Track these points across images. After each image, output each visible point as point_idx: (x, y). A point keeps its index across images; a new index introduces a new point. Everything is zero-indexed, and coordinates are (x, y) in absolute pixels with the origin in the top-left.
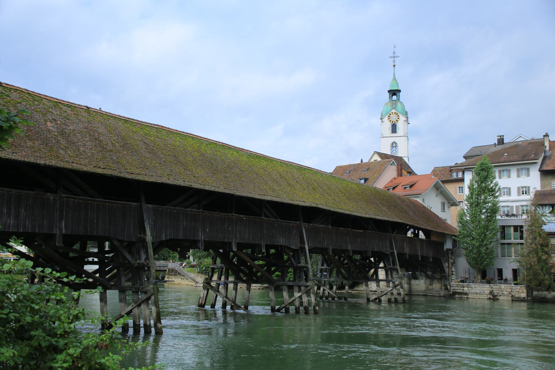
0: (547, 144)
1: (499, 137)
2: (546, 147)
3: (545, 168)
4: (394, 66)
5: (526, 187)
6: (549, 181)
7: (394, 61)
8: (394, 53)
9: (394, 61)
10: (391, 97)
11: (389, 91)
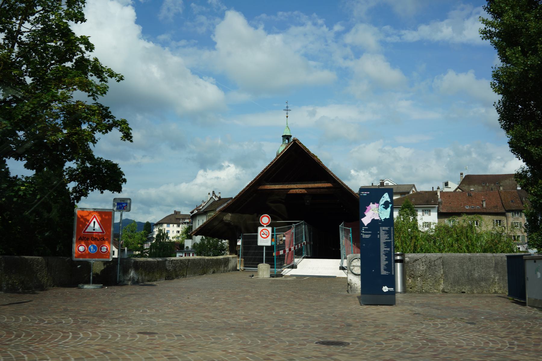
0: (439, 194)
1: (381, 181)
2: (438, 196)
3: (441, 211)
4: (287, 117)
5: (428, 223)
6: (443, 219)
7: (287, 114)
8: (287, 107)
9: (287, 114)
10: (284, 141)
11: (283, 136)
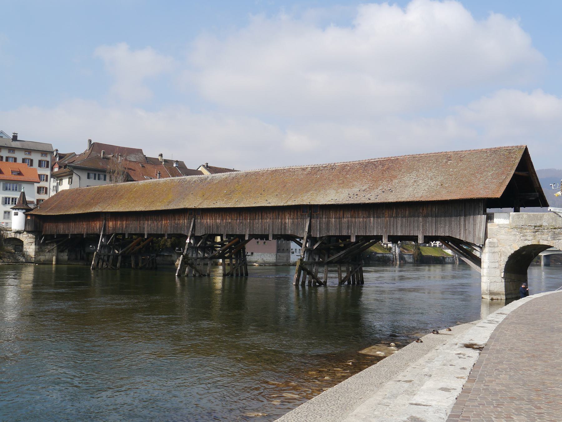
1: (14, 135)
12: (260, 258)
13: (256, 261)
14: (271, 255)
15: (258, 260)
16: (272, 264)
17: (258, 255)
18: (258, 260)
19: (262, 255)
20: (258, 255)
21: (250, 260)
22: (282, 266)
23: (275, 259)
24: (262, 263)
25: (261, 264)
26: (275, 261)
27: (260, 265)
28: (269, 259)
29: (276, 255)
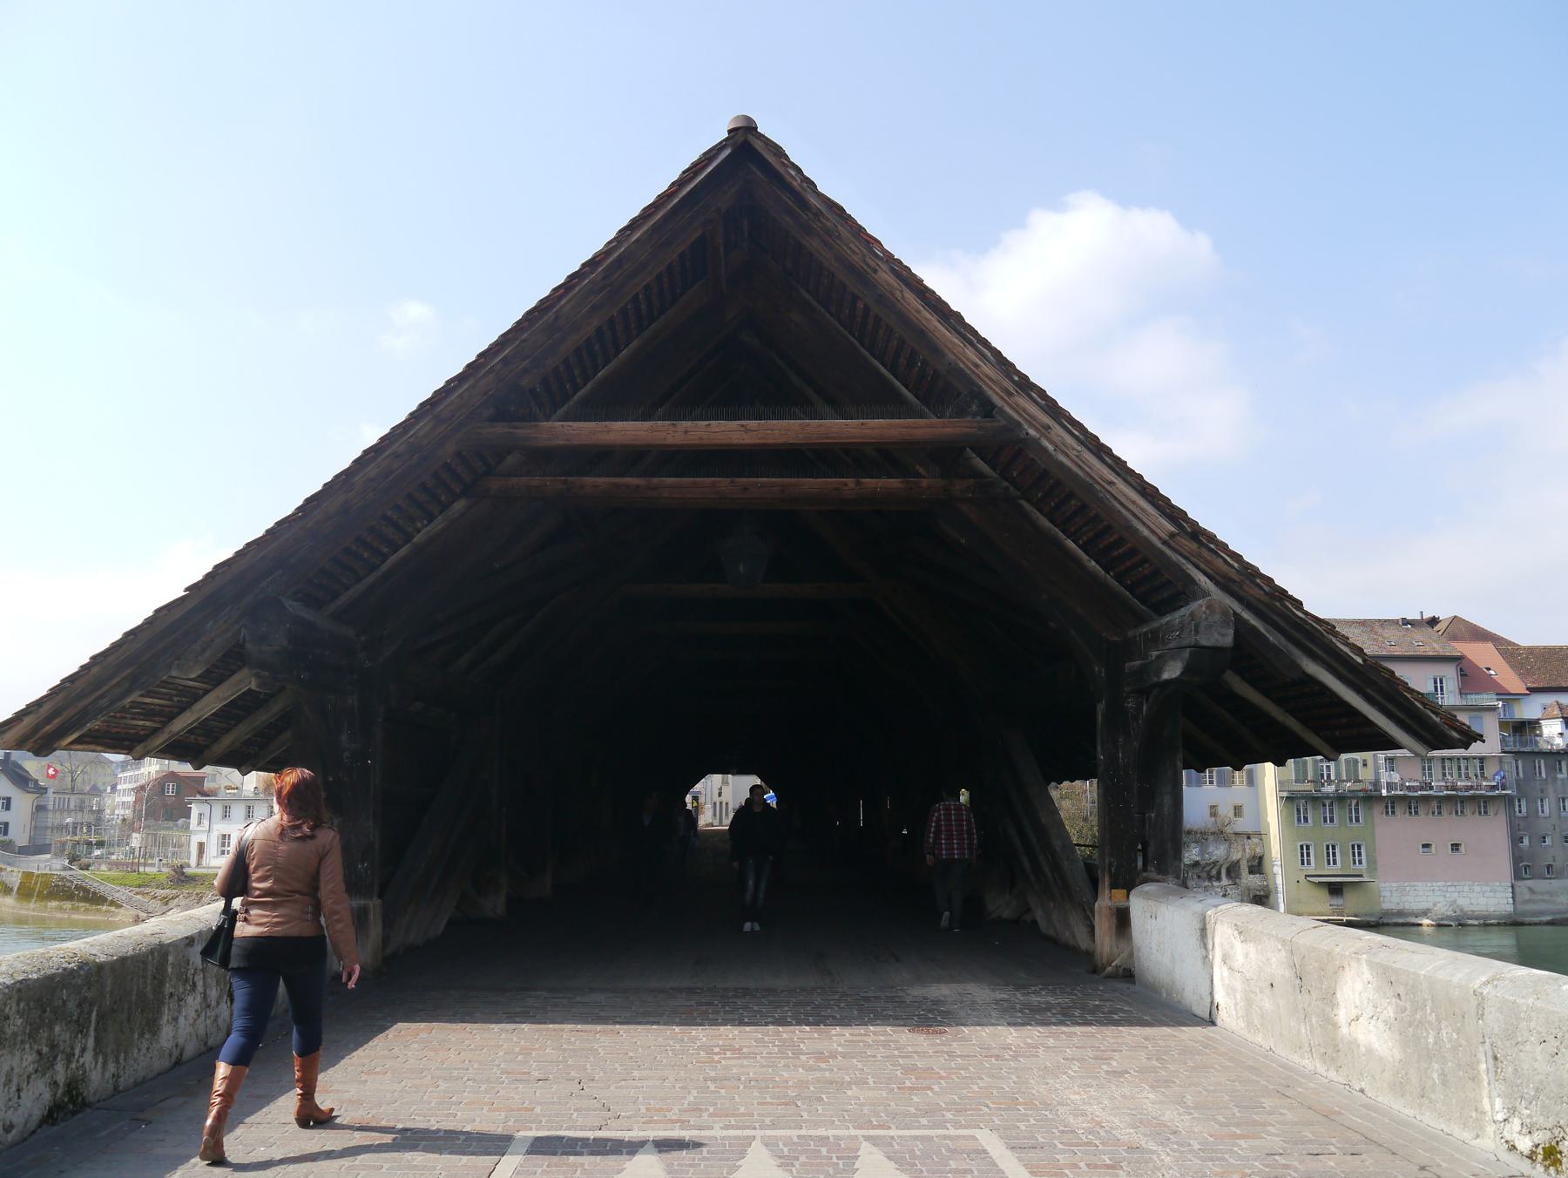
12: (1441, 899)
13: (1428, 909)
14: (1488, 889)
15: (1435, 905)
16: (1500, 917)
17: (1433, 890)
18: (1435, 905)
19: (1450, 889)
20: (1433, 890)
21: (1401, 907)
22: (1550, 928)
23: (1511, 901)
24: (1449, 918)
25: (1442, 919)
26: (1510, 908)
27: (1439, 925)
28: (1483, 901)
29: (1513, 887)
